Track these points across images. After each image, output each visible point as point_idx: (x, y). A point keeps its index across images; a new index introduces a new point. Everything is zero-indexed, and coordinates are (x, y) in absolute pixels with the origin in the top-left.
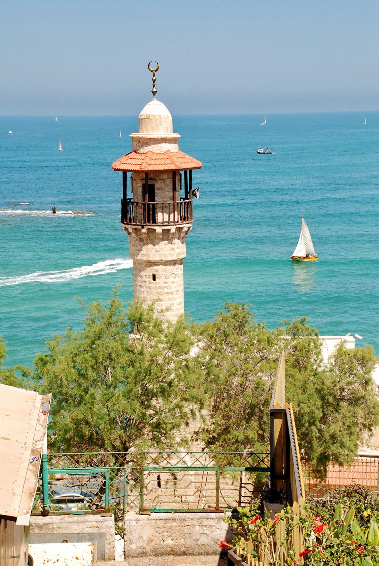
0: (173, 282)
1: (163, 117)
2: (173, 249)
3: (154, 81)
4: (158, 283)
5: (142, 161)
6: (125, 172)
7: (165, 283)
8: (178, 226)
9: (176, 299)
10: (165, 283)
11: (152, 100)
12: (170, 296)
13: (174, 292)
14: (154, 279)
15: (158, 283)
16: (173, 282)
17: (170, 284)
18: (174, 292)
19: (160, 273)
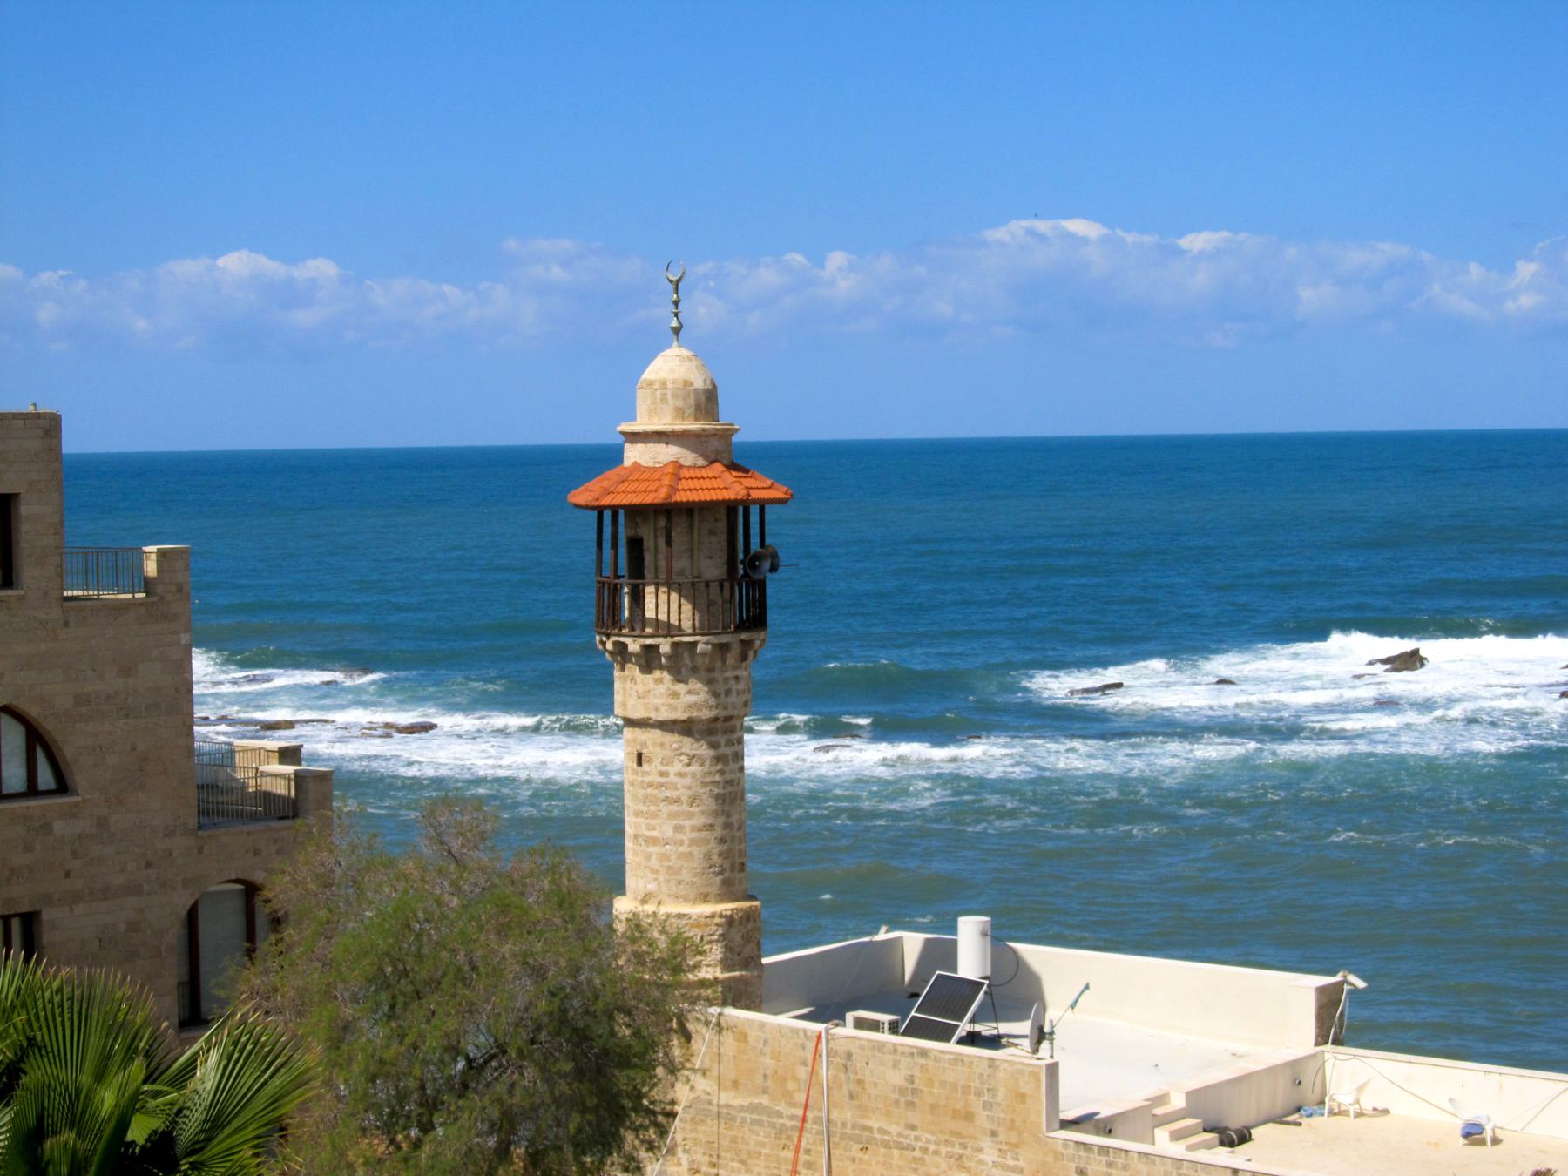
0: (680, 775)
1: (670, 385)
2: (675, 695)
3: (676, 303)
4: (648, 773)
5: (657, 484)
6: (600, 510)
7: (662, 774)
8: (676, 639)
9: (691, 816)
10: (662, 774)
11: (669, 346)
12: (675, 808)
13: (684, 799)
14: (640, 763)
15: (648, 773)
16: (680, 775)
17: (673, 778)
18: (684, 799)
19: (651, 749)
